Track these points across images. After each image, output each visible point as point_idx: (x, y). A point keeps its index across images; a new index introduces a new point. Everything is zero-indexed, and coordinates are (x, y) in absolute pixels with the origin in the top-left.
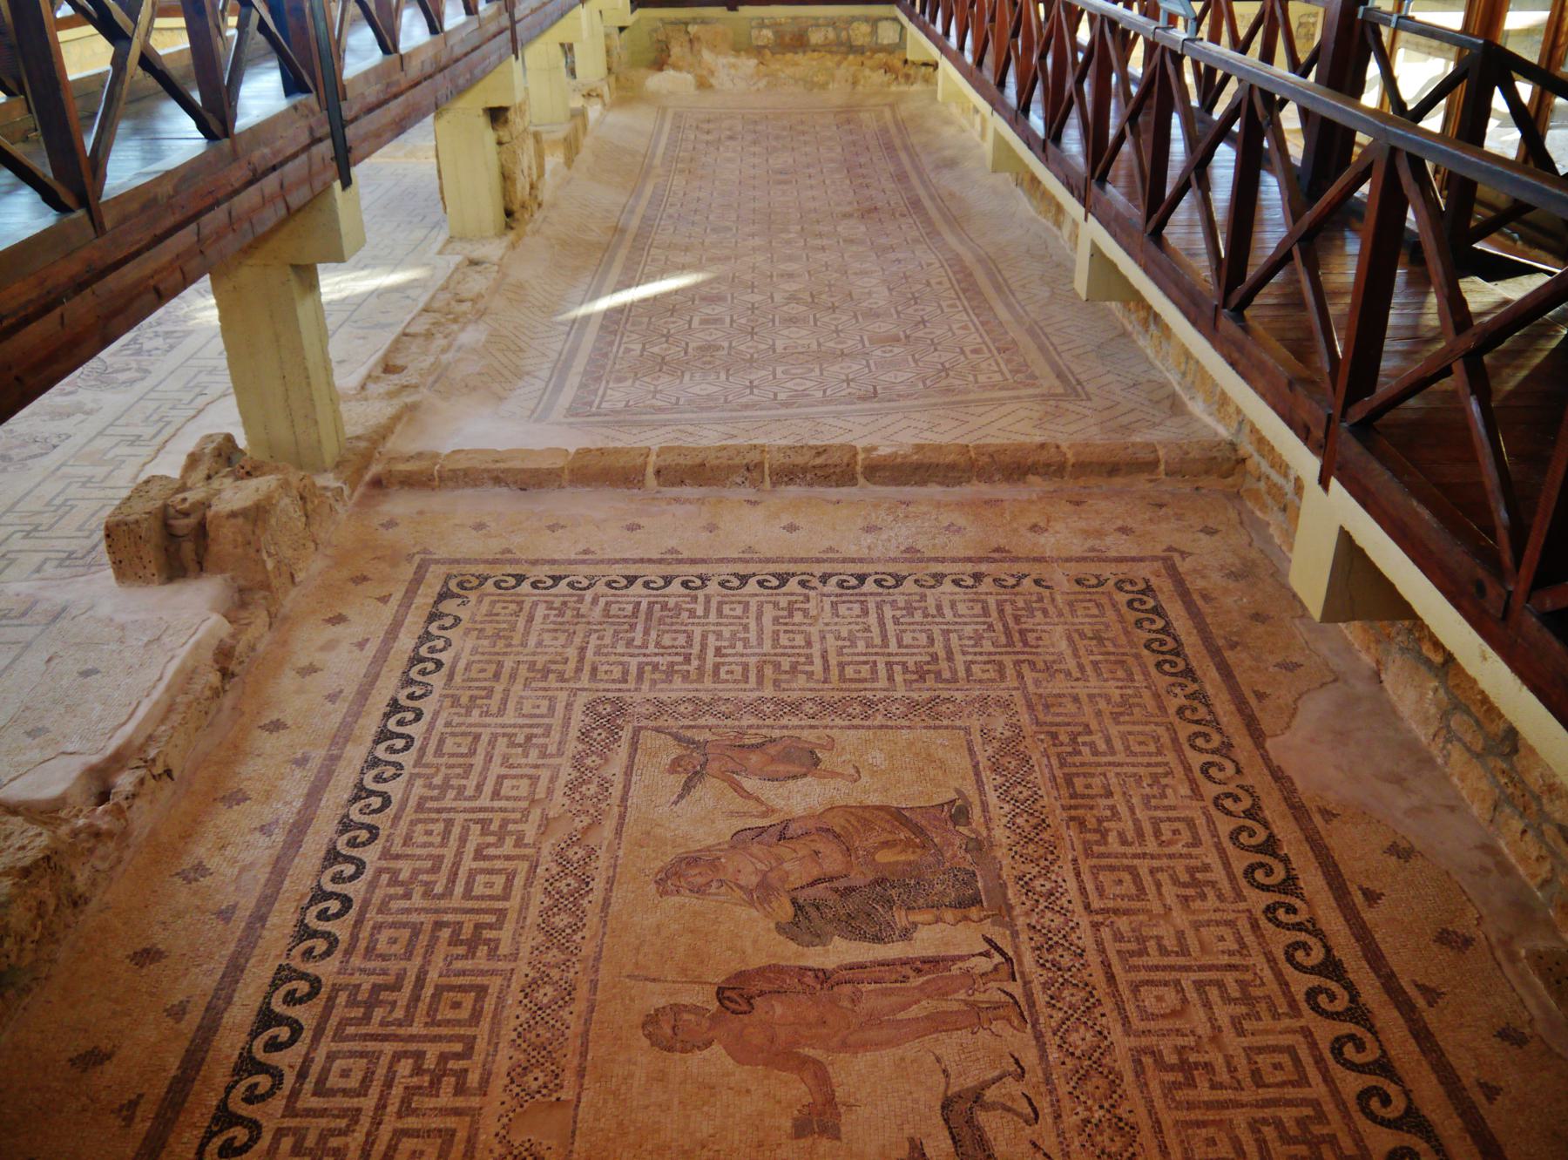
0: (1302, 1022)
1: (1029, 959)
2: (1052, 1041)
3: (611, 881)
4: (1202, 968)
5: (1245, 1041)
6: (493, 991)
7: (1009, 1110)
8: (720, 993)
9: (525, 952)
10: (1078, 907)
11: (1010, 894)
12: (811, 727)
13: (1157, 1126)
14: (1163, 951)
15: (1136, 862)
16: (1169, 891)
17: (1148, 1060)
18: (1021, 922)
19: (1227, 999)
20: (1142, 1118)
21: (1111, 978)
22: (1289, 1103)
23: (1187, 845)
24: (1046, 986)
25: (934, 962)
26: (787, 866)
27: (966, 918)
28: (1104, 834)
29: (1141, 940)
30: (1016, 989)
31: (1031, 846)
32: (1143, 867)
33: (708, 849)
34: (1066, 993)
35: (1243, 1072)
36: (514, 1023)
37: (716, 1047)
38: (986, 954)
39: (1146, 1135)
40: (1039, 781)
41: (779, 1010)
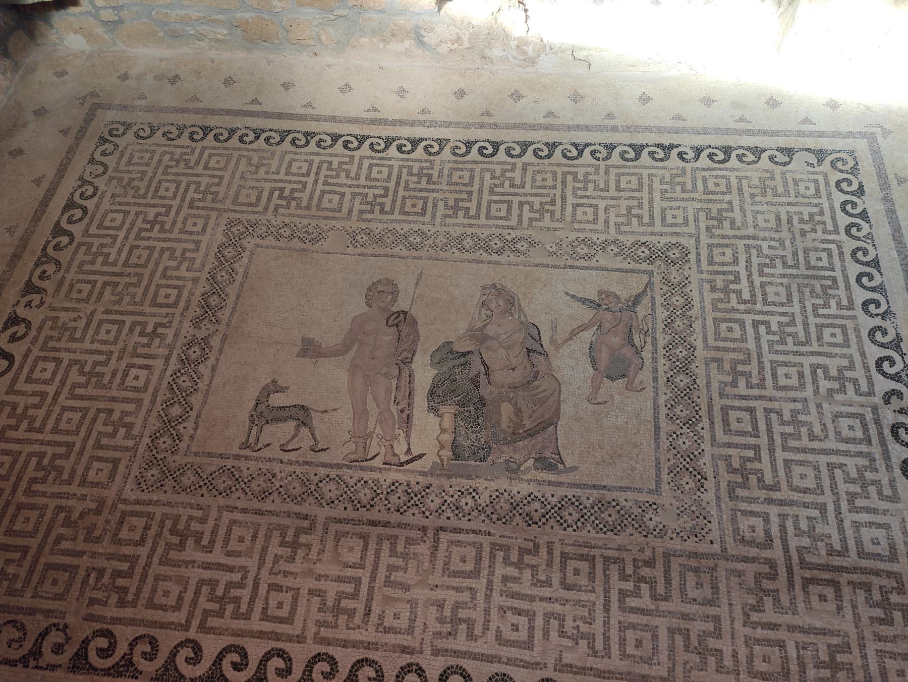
0: (309, 641)
3: (496, 263)
4: (371, 589)
6: (422, 219)
7: (293, 438)
8: (405, 313)
9: (447, 229)
10: (443, 522)
12: (655, 379)
14: (391, 568)
16: (451, 597)
17: (306, 524)
18: (435, 482)
19: (340, 596)
20: (267, 506)
21: (374, 523)
23: (499, 632)
24: (376, 482)
25: (408, 421)
26: (502, 352)
27: (442, 447)
28: (519, 565)
30: (378, 462)
31: (507, 506)
32: (480, 585)
33: (521, 310)
34: (368, 491)
36: (398, 229)
37: (367, 309)
38: (408, 451)
40: (585, 532)
41: (387, 338)
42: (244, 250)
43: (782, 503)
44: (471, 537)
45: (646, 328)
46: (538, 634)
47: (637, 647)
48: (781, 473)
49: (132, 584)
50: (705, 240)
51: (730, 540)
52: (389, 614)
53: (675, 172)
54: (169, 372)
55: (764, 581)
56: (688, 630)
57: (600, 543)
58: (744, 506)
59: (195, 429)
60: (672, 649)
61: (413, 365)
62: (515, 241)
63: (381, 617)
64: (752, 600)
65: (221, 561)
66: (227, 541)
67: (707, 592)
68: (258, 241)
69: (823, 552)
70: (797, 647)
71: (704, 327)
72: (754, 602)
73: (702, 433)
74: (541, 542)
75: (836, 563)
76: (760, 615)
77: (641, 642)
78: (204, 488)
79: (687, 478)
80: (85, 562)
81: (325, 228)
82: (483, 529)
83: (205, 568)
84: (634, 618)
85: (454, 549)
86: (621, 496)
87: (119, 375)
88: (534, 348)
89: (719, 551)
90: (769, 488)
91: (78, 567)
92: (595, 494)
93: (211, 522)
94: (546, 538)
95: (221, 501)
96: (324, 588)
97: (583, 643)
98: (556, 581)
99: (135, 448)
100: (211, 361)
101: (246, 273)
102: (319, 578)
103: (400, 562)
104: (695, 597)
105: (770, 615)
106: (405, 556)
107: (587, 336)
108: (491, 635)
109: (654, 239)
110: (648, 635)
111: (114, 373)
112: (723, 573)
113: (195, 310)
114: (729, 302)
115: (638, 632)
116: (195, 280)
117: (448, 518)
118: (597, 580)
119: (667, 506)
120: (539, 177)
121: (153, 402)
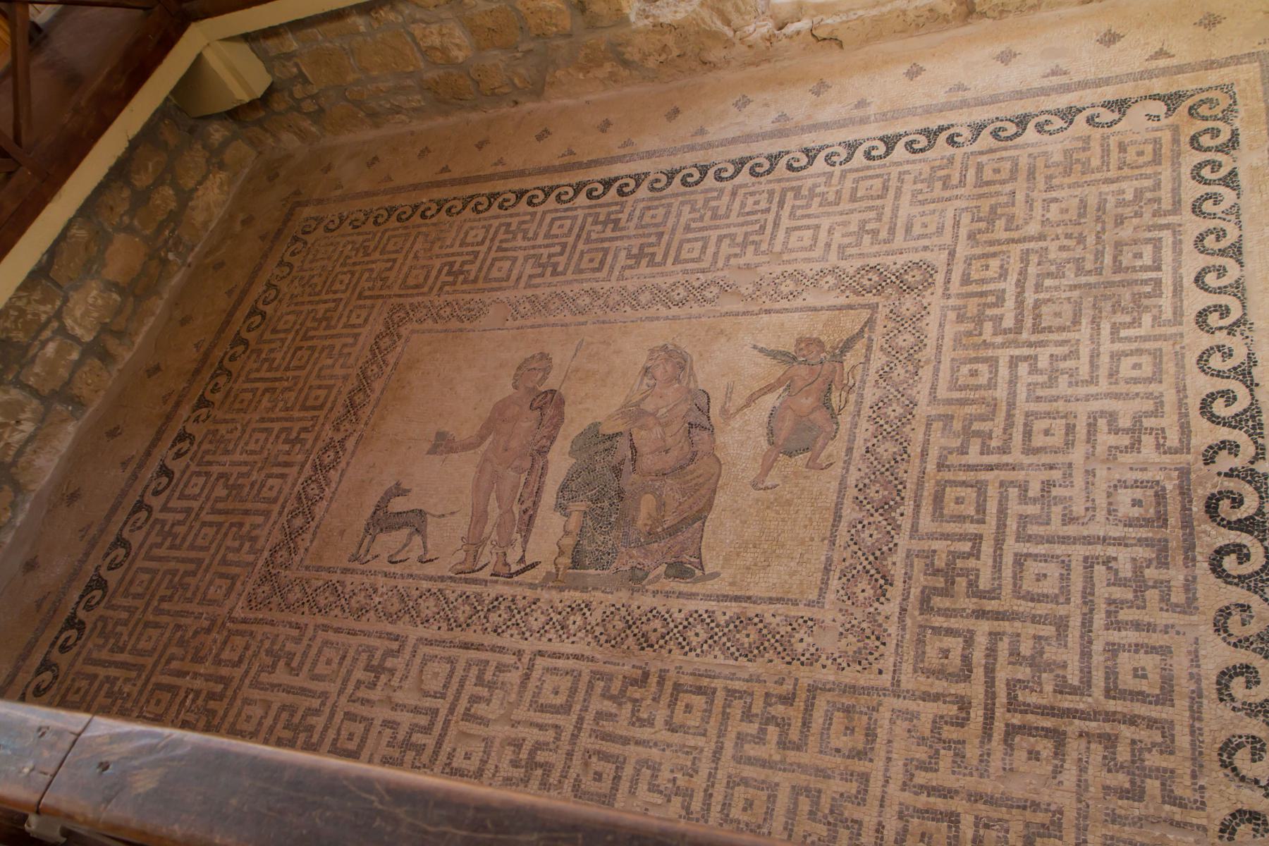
1: (507, 591)
2: (435, 586)
3: (674, 318)
4: (447, 723)
5: (377, 722)
7: (405, 545)
8: (553, 392)
10: (543, 645)
11: (578, 594)
12: (850, 450)
13: (352, 633)
14: (475, 699)
15: (574, 718)
16: (533, 735)
17: (395, 646)
18: (545, 595)
19: (414, 728)
20: (362, 625)
21: (466, 646)
22: (326, 729)
24: (479, 598)
26: (658, 430)
27: (561, 553)
28: (617, 699)
29: (491, 686)
30: (485, 574)
32: (567, 723)
34: (467, 608)
35: (357, 709)
37: (513, 390)
38: (522, 560)
39: (351, 623)
40: (709, 659)
42: (399, 337)
43: (998, 616)
44: (571, 663)
45: (851, 383)
46: (624, 786)
47: (745, 809)
48: (1007, 572)
49: (219, 707)
50: (962, 251)
51: (907, 668)
52: (460, 753)
53: (937, 163)
54: (300, 481)
55: (946, 728)
56: (819, 791)
57: (726, 672)
58: (938, 621)
59: (312, 542)
60: (792, 812)
61: (549, 456)
62: (703, 287)
63: (451, 756)
64: (921, 754)
65: (305, 685)
66: (315, 664)
67: (859, 741)
68: (417, 326)
69: (1049, 688)
70: (976, 825)
71: (936, 371)
72: (924, 757)
73: (900, 520)
74: (653, 670)
75: (1066, 705)
76: (930, 775)
77: (751, 805)
78: (307, 605)
79: (863, 584)
80: (186, 682)
81: (488, 302)
82: (586, 654)
83: (288, 692)
84: (749, 772)
85: (547, 677)
86: (767, 610)
87: (256, 487)
88: (699, 421)
89: (888, 685)
90: (982, 595)
91: (179, 687)
92: (733, 608)
93: (305, 642)
94: (660, 665)
95: (320, 620)
96: (398, 719)
97: (677, 801)
98: (659, 722)
99: (254, 565)
100: (343, 465)
101: (396, 364)
102: (395, 707)
103: (485, 692)
104: (840, 746)
105: (944, 776)
106: (491, 686)
107: (771, 400)
108: (567, 786)
109: (888, 260)
110: (763, 795)
111: (252, 485)
112: (888, 715)
113: (340, 410)
114: (981, 334)
115: (751, 790)
116: (346, 378)
117: (550, 640)
118: (712, 720)
119: (828, 622)
120: (750, 200)
121: (280, 513)
